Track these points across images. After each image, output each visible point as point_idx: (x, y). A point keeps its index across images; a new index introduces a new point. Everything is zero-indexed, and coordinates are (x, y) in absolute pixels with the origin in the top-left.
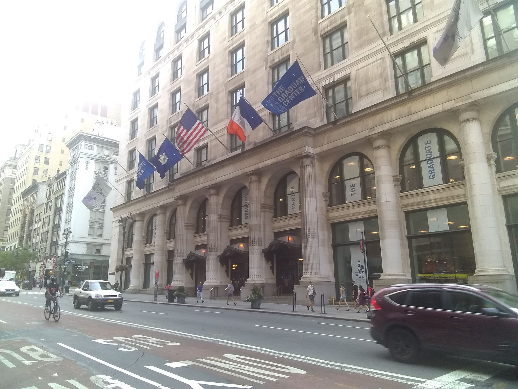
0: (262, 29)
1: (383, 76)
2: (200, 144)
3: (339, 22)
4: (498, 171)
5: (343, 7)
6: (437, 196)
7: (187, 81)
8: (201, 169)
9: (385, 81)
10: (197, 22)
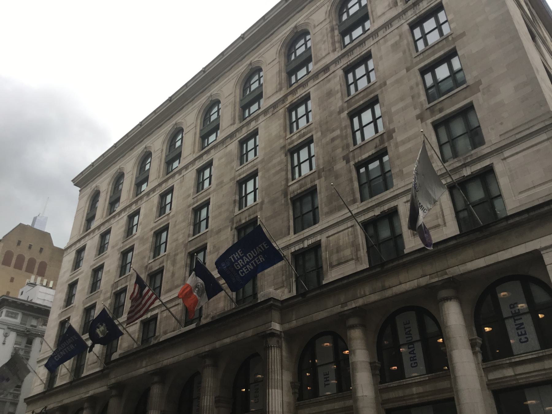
0: (229, 187)
1: (355, 246)
2: (149, 315)
3: (309, 186)
4: (484, 361)
5: (313, 171)
6: (420, 389)
7: (142, 240)
8: (148, 347)
9: (357, 251)
10: (161, 176)
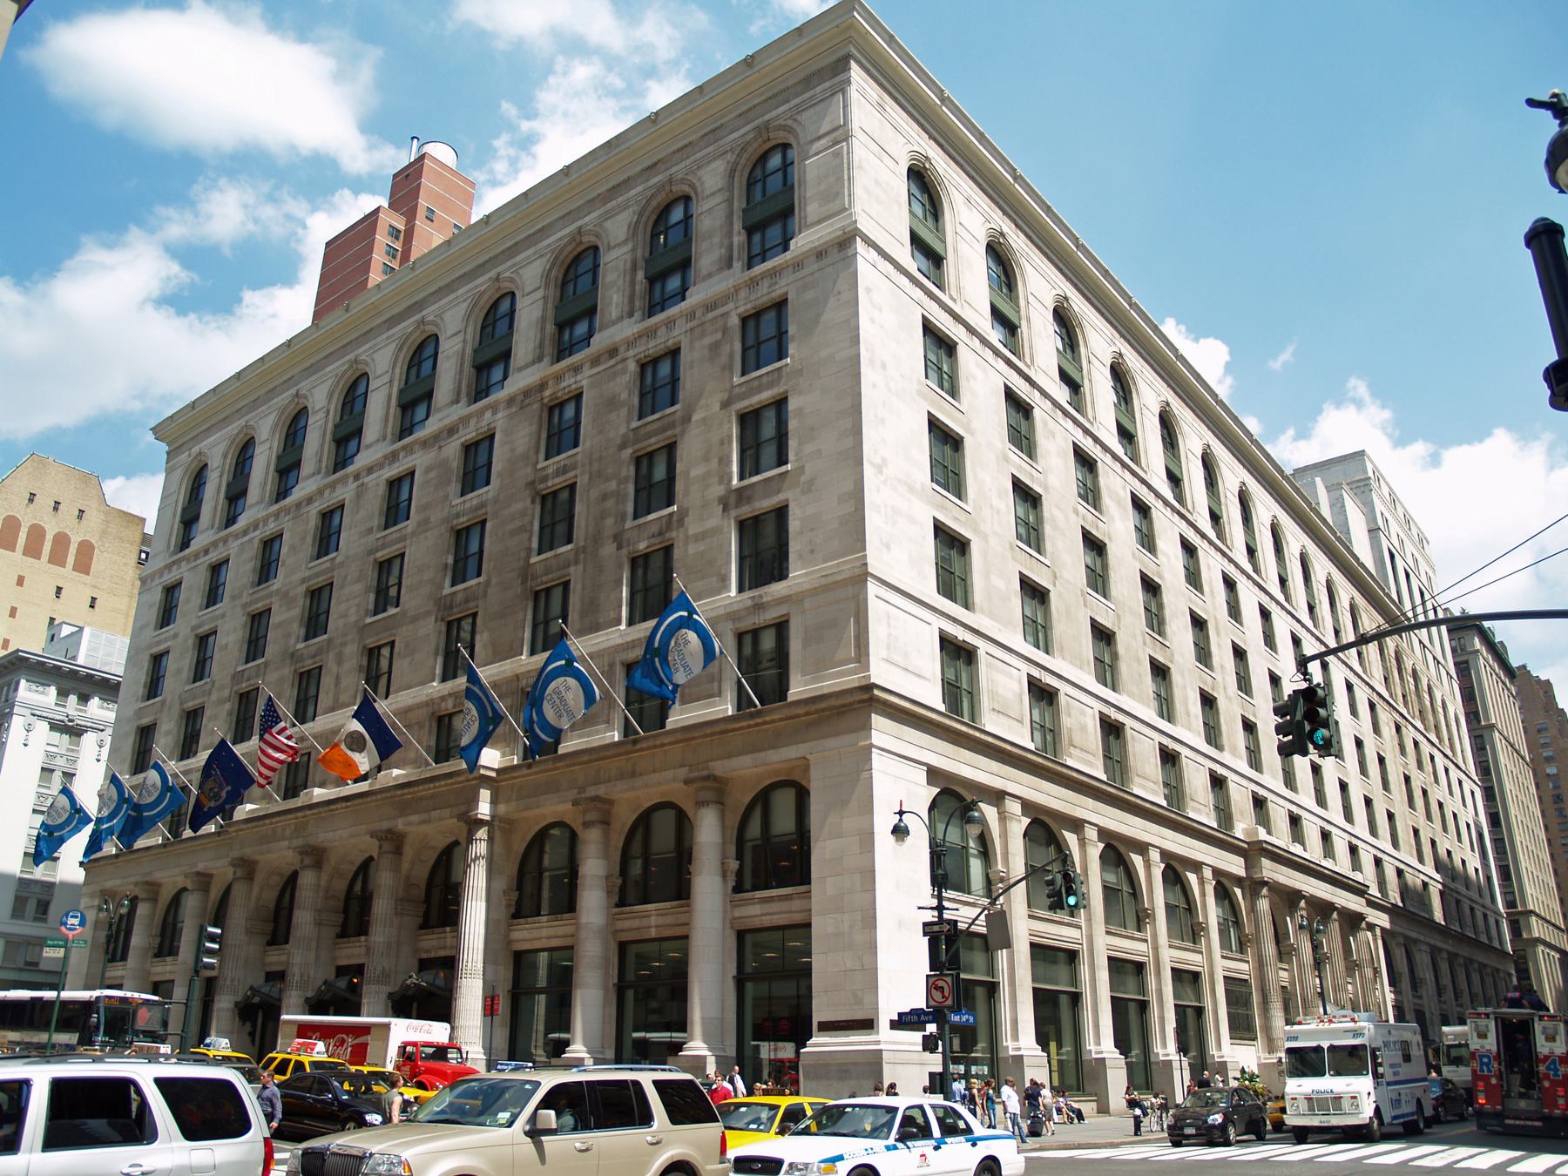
7: (286, 597)
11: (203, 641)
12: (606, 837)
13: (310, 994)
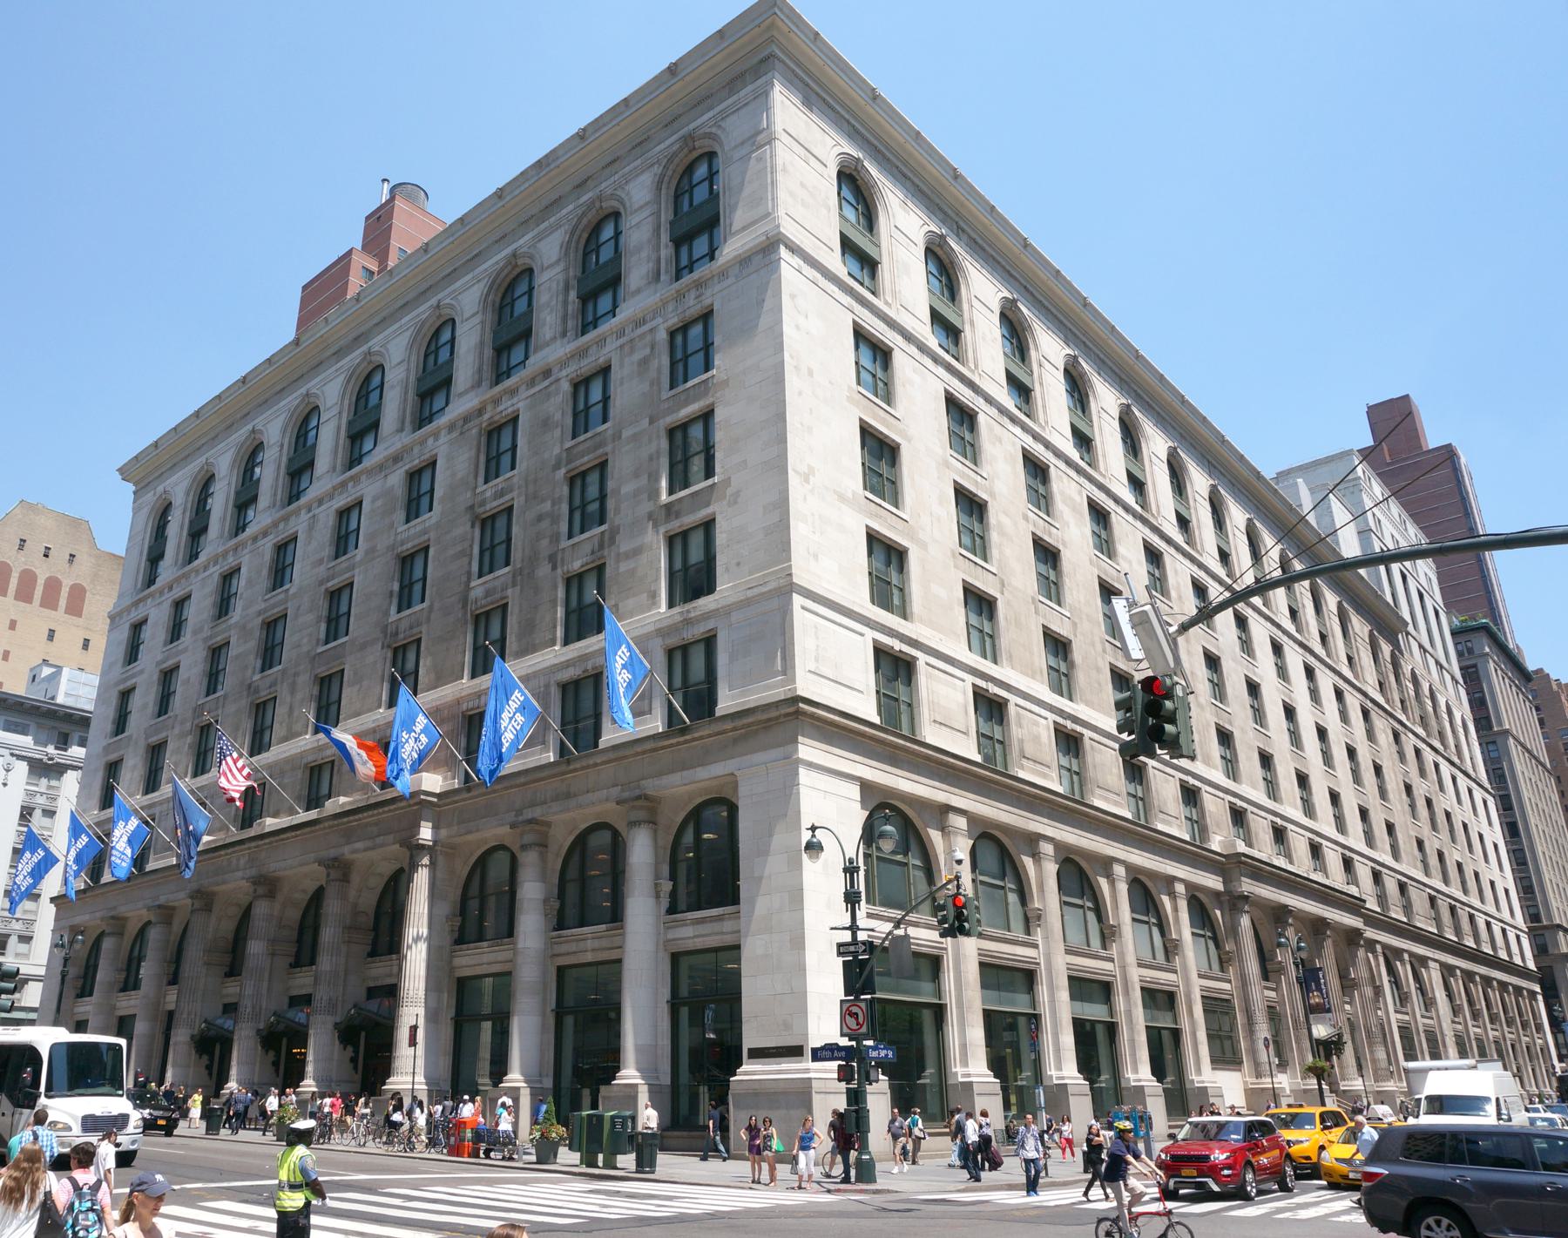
11: (168, 676)
12: (543, 859)
13: (262, 1026)
